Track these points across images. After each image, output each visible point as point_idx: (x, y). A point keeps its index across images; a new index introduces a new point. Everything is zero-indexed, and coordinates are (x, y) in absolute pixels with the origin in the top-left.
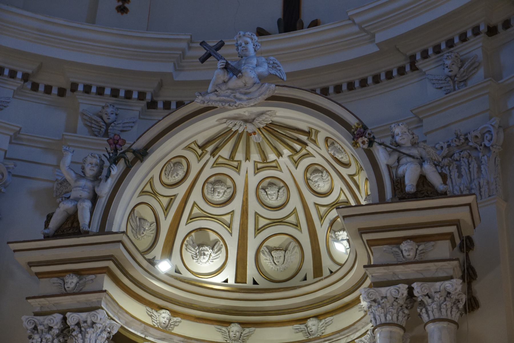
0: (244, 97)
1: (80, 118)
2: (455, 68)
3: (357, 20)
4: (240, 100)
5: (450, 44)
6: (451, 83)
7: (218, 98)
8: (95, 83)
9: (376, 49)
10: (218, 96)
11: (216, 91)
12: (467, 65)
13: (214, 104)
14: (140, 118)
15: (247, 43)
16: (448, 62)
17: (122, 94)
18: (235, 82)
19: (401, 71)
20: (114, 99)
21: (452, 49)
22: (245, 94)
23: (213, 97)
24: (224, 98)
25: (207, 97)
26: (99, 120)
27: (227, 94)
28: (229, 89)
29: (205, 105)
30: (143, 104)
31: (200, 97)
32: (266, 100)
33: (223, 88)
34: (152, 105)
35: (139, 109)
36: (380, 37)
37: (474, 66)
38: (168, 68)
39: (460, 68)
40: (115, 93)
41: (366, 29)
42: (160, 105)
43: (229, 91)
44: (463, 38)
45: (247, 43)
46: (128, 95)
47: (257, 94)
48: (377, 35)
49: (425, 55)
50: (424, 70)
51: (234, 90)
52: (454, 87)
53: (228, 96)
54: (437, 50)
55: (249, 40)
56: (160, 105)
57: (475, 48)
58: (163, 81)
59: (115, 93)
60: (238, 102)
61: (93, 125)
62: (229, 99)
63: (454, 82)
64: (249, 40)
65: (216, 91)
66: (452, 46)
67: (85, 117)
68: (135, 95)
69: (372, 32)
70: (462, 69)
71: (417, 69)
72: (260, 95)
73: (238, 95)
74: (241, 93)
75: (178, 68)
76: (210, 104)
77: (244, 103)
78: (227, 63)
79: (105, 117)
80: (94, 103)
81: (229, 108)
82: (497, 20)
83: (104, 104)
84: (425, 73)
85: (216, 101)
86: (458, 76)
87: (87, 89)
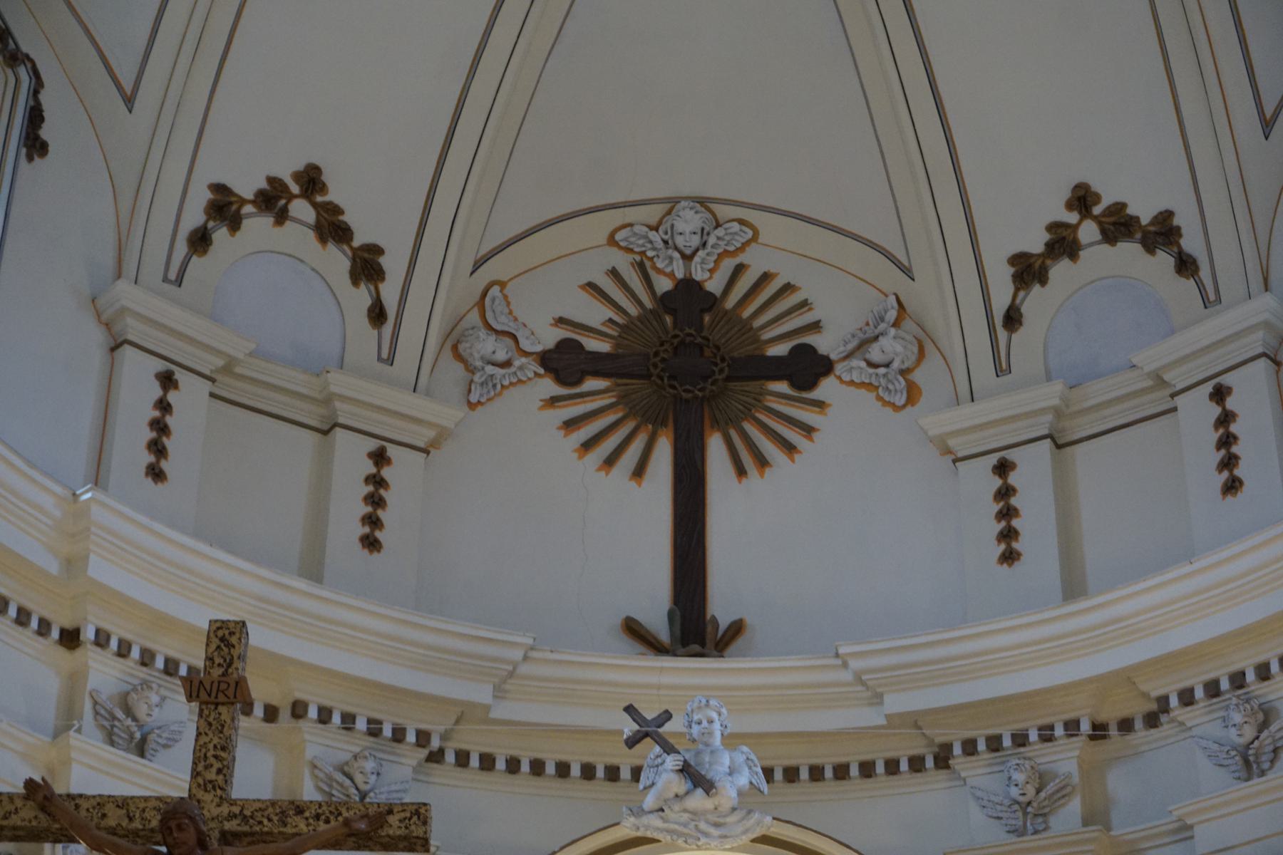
0: (713, 831)
1: (307, 772)
2: (1031, 791)
3: (855, 664)
4: (706, 835)
5: (1020, 740)
6: (1020, 814)
7: (666, 825)
8: (339, 706)
9: (883, 722)
10: (665, 820)
11: (663, 810)
12: (1051, 788)
13: (656, 835)
14: (414, 779)
15: (711, 722)
16: (1019, 777)
17: (387, 731)
18: (698, 800)
19: (917, 764)
20: (372, 739)
21: (1022, 749)
22: (717, 825)
23: (655, 821)
24: (676, 827)
25: (645, 820)
26: (348, 782)
27: (682, 820)
28: (685, 811)
29: (639, 834)
30: (423, 753)
31: (632, 819)
32: (753, 841)
33: (677, 807)
34: (436, 757)
35: (414, 763)
36: (897, 703)
37: (1064, 792)
38: (481, 693)
39: (1038, 791)
40: (374, 729)
41: (869, 683)
42: (450, 757)
43: (686, 816)
44: (1047, 735)
45: (711, 722)
46: (398, 735)
47: (740, 829)
48: (887, 698)
49: (970, 747)
50: (963, 774)
51: (694, 813)
52: (1025, 823)
53: (685, 825)
54: (994, 743)
55: (715, 715)
56: (450, 757)
57: (1065, 758)
58: (465, 713)
59: (374, 729)
60: (703, 840)
61: (334, 792)
62: (686, 831)
63: (1025, 814)
64: (715, 715)
65: (663, 810)
66: (1023, 745)
67: (316, 771)
68: (411, 737)
69: (879, 690)
70: (1043, 795)
71: (948, 767)
72: (745, 832)
73: (703, 826)
74: (707, 822)
75: (500, 692)
76: (649, 834)
77: (713, 844)
78: (685, 761)
79: (359, 779)
80: (329, 743)
81: (684, 845)
82: (1110, 714)
83: (357, 750)
84: (964, 779)
85: (662, 830)
86: (1035, 804)
87: (325, 716)
